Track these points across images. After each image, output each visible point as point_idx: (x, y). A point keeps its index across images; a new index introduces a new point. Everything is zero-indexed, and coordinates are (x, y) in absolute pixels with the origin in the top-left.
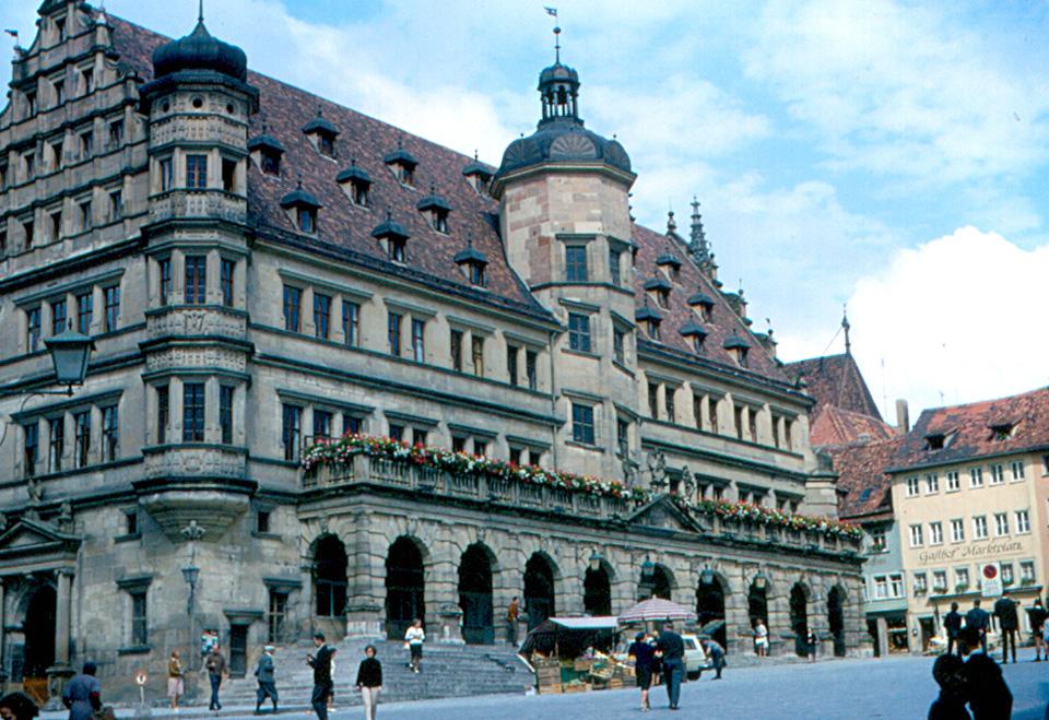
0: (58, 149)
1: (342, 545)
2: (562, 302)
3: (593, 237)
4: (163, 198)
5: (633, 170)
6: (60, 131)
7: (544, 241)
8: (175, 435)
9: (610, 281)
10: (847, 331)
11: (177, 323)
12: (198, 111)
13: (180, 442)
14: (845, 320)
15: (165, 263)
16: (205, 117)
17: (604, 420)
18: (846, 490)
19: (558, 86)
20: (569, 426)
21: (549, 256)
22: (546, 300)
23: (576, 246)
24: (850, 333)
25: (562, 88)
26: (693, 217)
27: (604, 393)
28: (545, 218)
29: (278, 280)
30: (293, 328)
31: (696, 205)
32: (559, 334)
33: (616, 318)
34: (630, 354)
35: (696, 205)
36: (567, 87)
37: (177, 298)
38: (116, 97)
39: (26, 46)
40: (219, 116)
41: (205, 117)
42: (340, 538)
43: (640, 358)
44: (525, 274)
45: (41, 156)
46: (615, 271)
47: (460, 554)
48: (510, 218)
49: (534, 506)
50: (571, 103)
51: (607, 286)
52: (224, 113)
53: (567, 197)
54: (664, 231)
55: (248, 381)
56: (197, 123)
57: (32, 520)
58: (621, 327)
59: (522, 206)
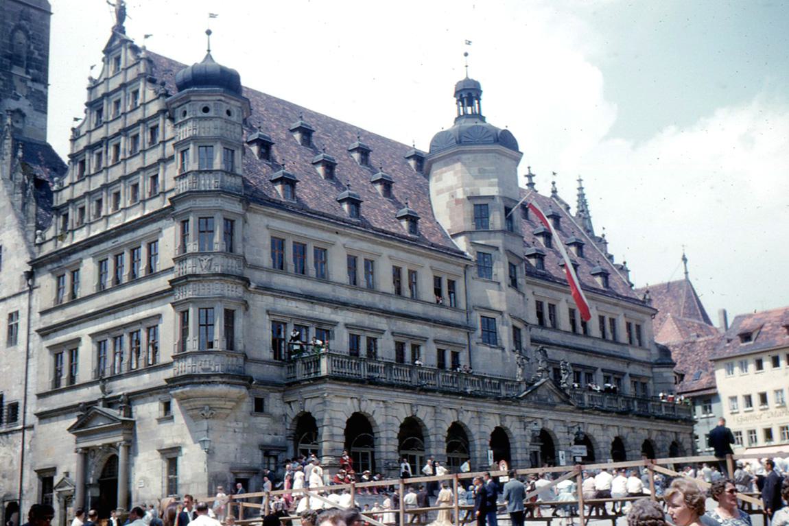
0: (117, 147)
1: (314, 420)
3: (493, 197)
4: (183, 178)
5: (520, 150)
6: (117, 135)
7: (458, 201)
8: (192, 345)
10: (685, 263)
12: (205, 115)
13: (197, 350)
14: (684, 256)
15: (185, 223)
16: (211, 118)
18: (683, 373)
19: (469, 93)
24: (687, 265)
25: (470, 94)
26: (578, 189)
30: (280, 266)
31: (580, 181)
35: (580, 181)
36: (474, 95)
37: (192, 247)
38: (153, 108)
39: (96, 77)
40: (220, 118)
42: (313, 415)
44: (446, 224)
45: (107, 152)
47: (399, 424)
49: (351, 375)
50: (477, 105)
52: (225, 115)
54: (548, 194)
55: (246, 305)
57: (100, 407)
59: (444, 179)
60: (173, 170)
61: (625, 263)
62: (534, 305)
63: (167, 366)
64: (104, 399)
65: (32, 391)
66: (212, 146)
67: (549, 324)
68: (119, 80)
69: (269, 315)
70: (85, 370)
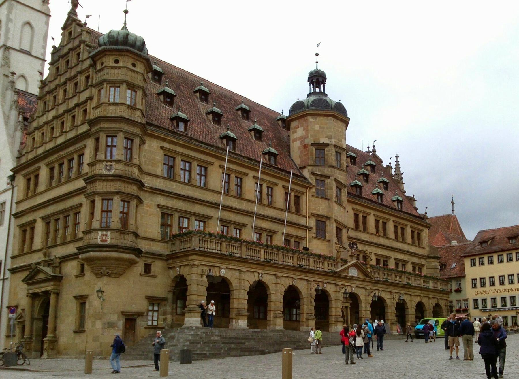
2: (313, 174)
3: (327, 145)
7: (305, 146)
9: (334, 164)
11: (101, 169)
16: (119, 68)
17: (331, 228)
20: (314, 231)
21: (308, 154)
22: (306, 173)
23: (320, 147)
27: (330, 215)
28: (306, 136)
29: (162, 152)
32: (311, 188)
33: (336, 181)
34: (344, 197)
41: (119, 68)
43: (349, 201)
44: (298, 161)
46: (339, 160)
48: (293, 136)
51: (333, 167)
53: (317, 127)
56: (116, 71)
57: (41, 267)
58: (340, 185)
60: (94, 104)
61: (414, 196)
62: (353, 216)
63: (81, 239)
64: (45, 261)
65: (10, 254)
66: (119, 87)
67: (362, 229)
68: (70, 46)
69: (159, 207)
70: (38, 242)
